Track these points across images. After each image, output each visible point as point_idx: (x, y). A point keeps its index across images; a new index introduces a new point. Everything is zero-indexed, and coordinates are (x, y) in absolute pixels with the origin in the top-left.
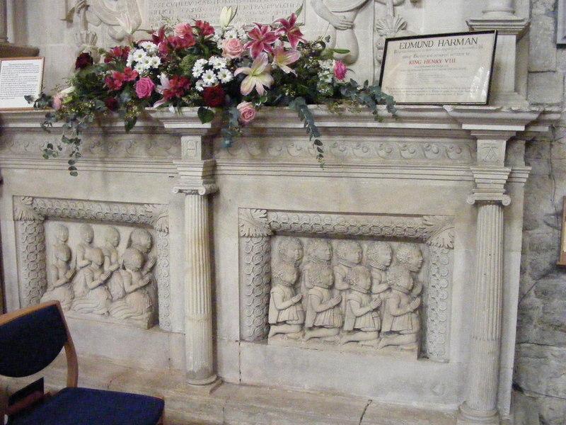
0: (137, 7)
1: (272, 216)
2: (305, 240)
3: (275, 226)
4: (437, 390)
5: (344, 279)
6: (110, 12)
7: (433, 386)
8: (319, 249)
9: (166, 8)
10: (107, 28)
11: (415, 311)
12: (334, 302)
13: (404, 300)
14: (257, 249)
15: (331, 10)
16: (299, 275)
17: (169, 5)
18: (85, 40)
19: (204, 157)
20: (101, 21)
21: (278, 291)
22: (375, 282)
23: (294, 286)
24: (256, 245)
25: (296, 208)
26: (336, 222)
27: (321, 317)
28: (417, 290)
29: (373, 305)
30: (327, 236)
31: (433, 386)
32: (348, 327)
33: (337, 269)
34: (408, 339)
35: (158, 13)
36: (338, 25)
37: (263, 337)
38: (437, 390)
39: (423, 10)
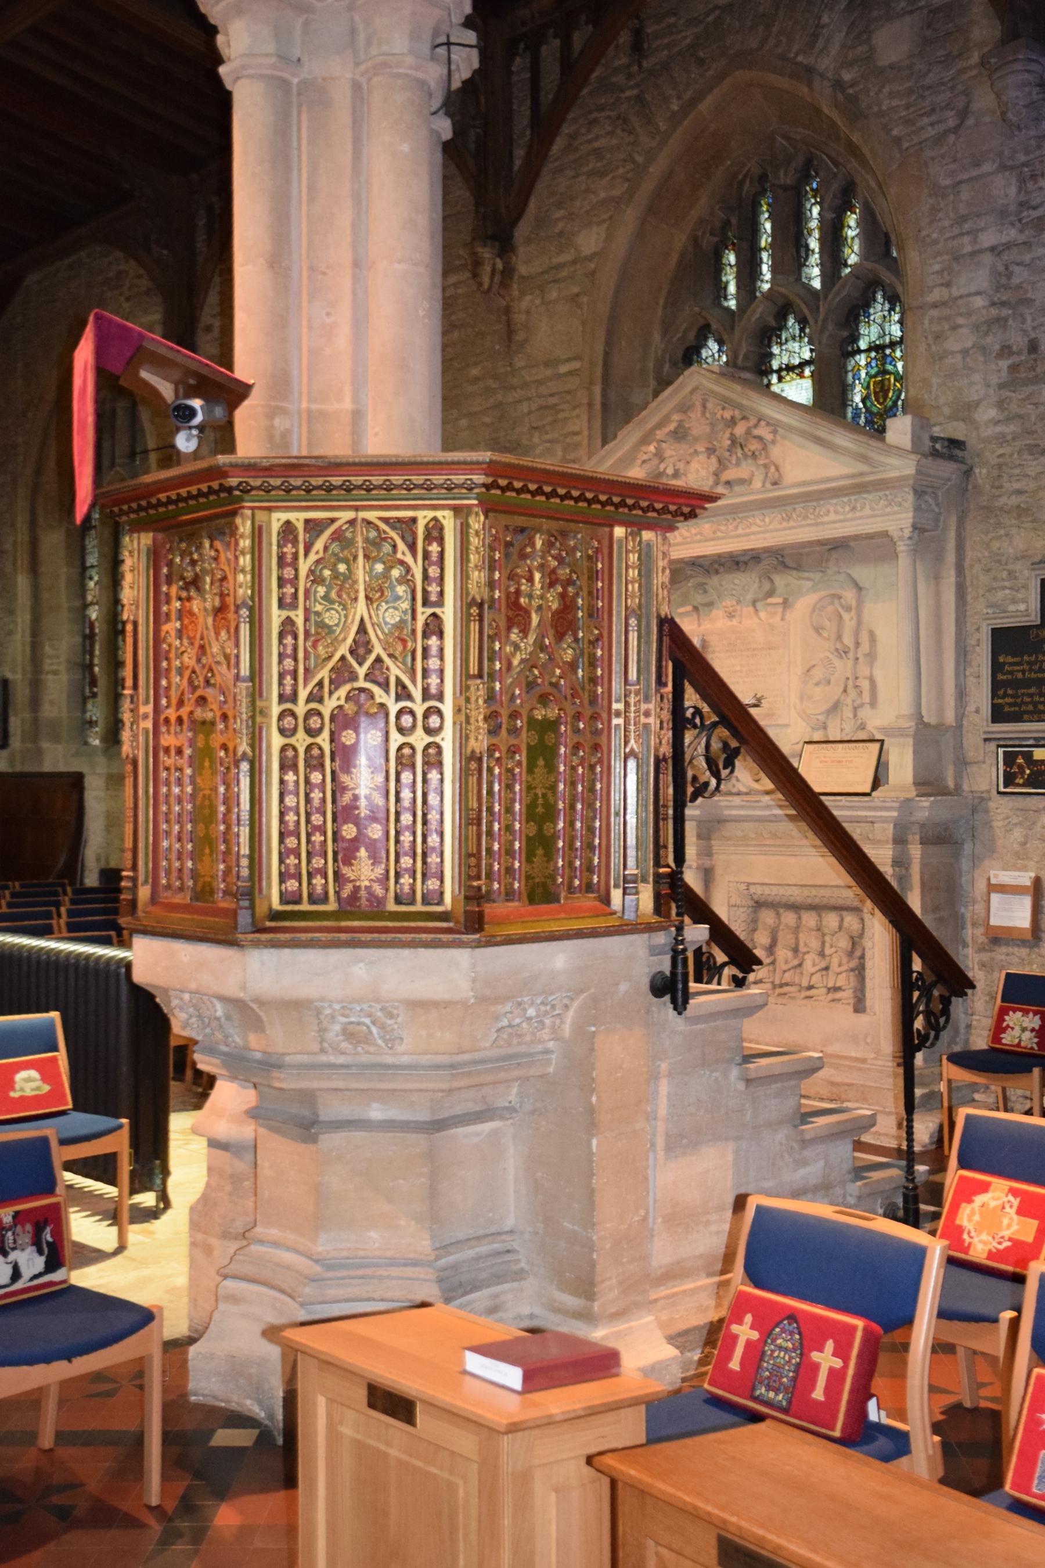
1: (753, 889)
2: (781, 911)
3: (756, 897)
4: (869, 1040)
5: (806, 945)
7: (866, 1037)
8: (789, 918)
11: (852, 970)
12: (796, 962)
13: (845, 960)
14: (743, 917)
22: (827, 945)
25: (766, 881)
26: (795, 895)
27: (787, 975)
28: (858, 954)
29: (823, 965)
30: (795, 907)
31: (866, 1037)
32: (805, 984)
33: (801, 935)
34: (847, 995)
38: (869, 1040)
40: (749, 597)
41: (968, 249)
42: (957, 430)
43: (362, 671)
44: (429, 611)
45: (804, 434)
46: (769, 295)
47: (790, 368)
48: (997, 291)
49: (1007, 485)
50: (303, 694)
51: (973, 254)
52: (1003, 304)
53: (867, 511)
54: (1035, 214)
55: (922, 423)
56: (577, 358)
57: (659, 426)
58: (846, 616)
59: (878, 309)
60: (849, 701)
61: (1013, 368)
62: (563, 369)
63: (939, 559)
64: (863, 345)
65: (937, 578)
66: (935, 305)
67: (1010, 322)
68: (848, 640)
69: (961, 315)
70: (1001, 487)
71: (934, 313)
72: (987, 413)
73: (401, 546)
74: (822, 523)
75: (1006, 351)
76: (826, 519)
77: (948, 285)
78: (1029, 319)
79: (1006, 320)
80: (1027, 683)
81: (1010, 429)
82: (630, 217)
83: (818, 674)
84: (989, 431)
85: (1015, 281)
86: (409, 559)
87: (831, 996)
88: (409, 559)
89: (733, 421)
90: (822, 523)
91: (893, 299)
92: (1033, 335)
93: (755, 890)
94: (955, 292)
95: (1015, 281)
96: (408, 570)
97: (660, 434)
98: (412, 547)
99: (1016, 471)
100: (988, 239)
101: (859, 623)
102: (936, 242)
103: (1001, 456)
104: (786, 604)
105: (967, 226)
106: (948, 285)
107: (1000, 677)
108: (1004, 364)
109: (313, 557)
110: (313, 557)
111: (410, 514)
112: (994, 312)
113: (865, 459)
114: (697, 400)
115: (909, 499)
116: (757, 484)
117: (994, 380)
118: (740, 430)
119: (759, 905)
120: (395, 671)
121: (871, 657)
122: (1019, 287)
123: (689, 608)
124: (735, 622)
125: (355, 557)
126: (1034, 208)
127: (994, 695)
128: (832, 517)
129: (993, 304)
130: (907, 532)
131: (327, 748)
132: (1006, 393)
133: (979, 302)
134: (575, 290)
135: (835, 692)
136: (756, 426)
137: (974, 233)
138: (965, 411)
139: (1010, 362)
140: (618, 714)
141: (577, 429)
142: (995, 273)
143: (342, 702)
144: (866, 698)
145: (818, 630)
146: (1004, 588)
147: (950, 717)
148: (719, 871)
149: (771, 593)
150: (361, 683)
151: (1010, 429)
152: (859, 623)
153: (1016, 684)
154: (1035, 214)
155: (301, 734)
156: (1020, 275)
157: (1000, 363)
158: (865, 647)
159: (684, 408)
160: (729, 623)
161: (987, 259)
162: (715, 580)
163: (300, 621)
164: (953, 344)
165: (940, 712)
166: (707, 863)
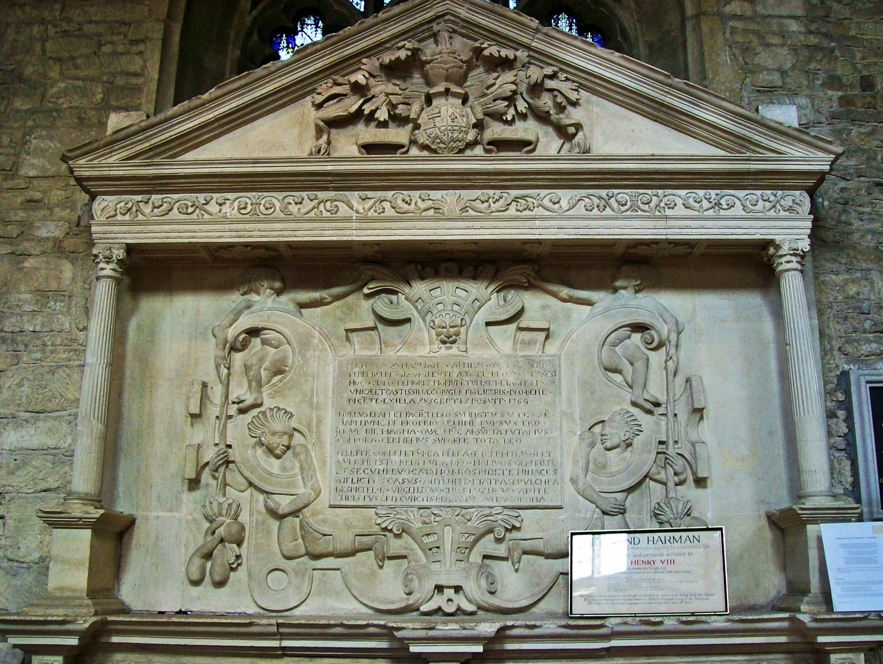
0: (315, 471)
6: (270, 474)
9: (363, 475)
10: (261, 497)
15: (597, 490)
17: (366, 471)
18: (224, 512)
20: (251, 484)
35: (350, 481)
36: (607, 508)
39: (708, 491)
48: (812, 21)
49: (856, 224)
52: (826, 35)
53: (738, 211)
61: (845, 101)
66: (735, 17)
67: (837, 53)
69: (774, 33)
70: (850, 224)
71: (739, 25)
74: (667, 218)
75: (833, 82)
76: (669, 212)
78: (859, 56)
79: (832, 50)
90: (667, 218)
92: (865, 73)
97: (370, 64)
99: (867, 210)
103: (843, 190)
112: (814, 40)
122: (839, 22)
124: (455, 350)
128: (680, 211)
133: (794, 26)
136: (553, 76)
139: (840, 93)
141: (135, 68)
146: (869, 341)
157: (830, 93)
160: (443, 351)
162: (420, 288)
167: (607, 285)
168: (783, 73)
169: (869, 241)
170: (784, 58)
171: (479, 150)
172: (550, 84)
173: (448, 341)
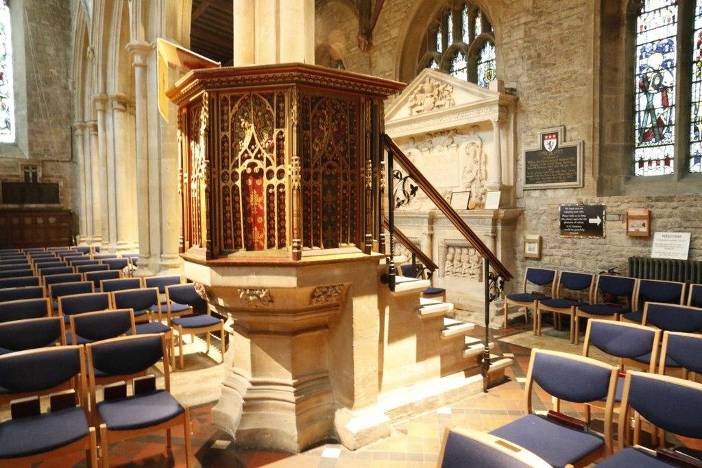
8: (458, 250)
12: (460, 265)
13: (476, 264)
16: (453, 258)
19: (429, 224)
21: (448, 262)
23: (452, 261)
24: (443, 249)
37: (444, 277)
40: (446, 144)
41: (516, 24)
42: (513, 85)
43: (253, 155)
44: (279, 130)
45: (463, 89)
46: (452, 47)
47: (459, 70)
49: (531, 103)
50: (230, 168)
51: (519, 25)
52: (529, 42)
53: (483, 113)
54: (538, 11)
55: (501, 83)
56: (391, 70)
57: (415, 89)
58: (477, 150)
59: (488, 47)
60: (478, 178)
61: (532, 63)
62: (387, 74)
63: (507, 129)
64: (483, 60)
65: (507, 135)
66: (505, 44)
68: (478, 158)
72: (524, 79)
73: (268, 104)
75: (530, 57)
77: (510, 37)
80: (538, 170)
81: (532, 84)
82: (407, 24)
83: (468, 169)
84: (524, 85)
85: (532, 34)
86: (271, 109)
87: (472, 276)
88: (271, 109)
89: (438, 86)
91: (492, 45)
93: (448, 242)
94: (512, 39)
95: (532, 34)
96: (271, 114)
97: (416, 91)
98: (272, 105)
100: (523, 20)
101: (481, 152)
102: (505, 23)
104: (458, 146)
105: (515, 17)
106: (510, 37)
107: (529, 168)
108: (529, 62)
109: (234, 111)
110: (234, 111)
111: (271, 91)
113: (481, 96)
114: (427, 79)
115: (497, 108)
116: (447, 106)
117: (526, 67)
118: (441, 88)
119: (448, 247)
120: (266, 155)
121: (486, 163)
123: (426, 149)
125: (250, 110)
126: (539, 9)
127: (527, 175)
128: (472, 116)
129: (525, 42)
130: (497, 120)
131: (240, 186)
132: (530, 72)
133: (520, 42)
134: (390, 48)
135: (472, 175)
137: (518, 19)
138: (516, 78)
140: (363, 172)
142: (525, 31)
143: (245, 168)
144: (484, 177)
145: (468, 154)
147: (512, 184)
148: (435, 236)
149: (453, 143)
150: (252, 160)
151: (532, 84)
152: (481, 152)
153: (534, 171)
154: (538, 11)
155: (230, 181)
156: (534, 31)
157: (528, 62)
158: (483, 160)
159: (423, 82)
161: (523, 27)
163: (229, 137)
164: (511, 56)
165: (509, 181)
166: (432, 232)
167: (467, 133)
168: (516, 59)
169: (532, 108)
170: (517, 54)
171: (435, 109)
172: (446, 89)
173: (440, 151)
